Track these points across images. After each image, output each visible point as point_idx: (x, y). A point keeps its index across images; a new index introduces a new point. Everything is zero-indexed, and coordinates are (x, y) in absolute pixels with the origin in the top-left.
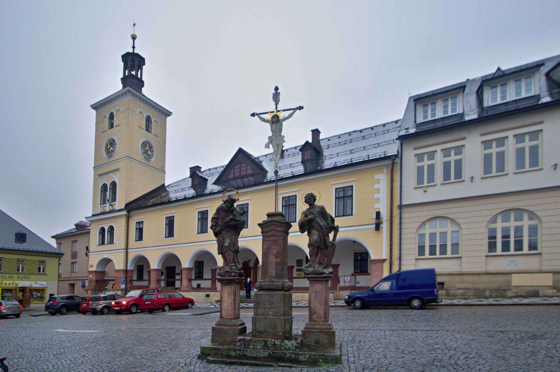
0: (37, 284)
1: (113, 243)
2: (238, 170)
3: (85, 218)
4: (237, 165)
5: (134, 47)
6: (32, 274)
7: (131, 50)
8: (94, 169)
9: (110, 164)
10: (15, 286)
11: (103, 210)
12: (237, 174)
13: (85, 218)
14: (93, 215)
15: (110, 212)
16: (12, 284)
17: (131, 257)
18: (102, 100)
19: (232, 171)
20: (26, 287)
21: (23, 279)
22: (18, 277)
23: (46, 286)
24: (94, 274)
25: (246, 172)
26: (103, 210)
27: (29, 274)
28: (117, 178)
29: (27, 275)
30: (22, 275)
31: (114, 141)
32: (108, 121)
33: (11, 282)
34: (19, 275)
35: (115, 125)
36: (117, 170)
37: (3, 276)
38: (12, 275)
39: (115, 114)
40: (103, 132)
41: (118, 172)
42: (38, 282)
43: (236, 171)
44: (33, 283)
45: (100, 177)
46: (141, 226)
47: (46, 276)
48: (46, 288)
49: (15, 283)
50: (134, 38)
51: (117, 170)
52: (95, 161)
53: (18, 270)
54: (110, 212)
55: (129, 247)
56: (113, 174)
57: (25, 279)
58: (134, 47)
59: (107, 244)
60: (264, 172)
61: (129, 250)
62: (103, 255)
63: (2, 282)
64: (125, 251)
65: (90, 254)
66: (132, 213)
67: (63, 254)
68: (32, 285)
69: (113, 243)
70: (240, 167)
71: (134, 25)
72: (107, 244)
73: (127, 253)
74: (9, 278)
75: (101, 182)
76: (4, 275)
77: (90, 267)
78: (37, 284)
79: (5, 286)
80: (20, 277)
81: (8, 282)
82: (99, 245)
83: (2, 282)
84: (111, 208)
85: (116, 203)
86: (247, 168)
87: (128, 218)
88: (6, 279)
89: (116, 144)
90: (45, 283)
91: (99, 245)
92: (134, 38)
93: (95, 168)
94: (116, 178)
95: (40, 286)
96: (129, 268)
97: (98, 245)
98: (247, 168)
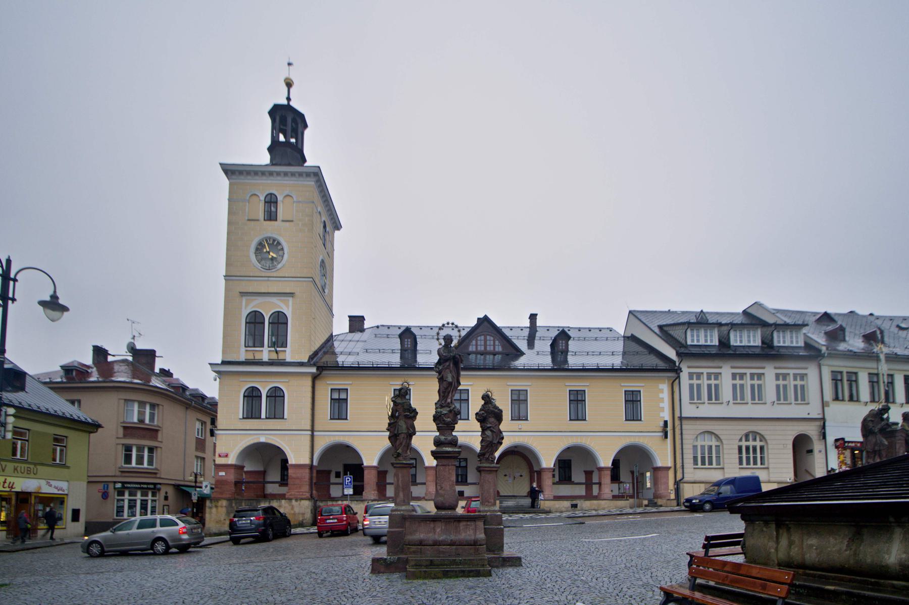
0: (51, 486)
1: (283, 418)
2: (483, 343)
3: (210, 364)
4: (481, 335)
6: (43, 464)
8: (225, 280)
9: (268, 280)
10: (8, 489)
11: (252, 358)
13: (210, 364)
14: (224, 363)
15: (271, 363)
17: (322, 444)
18: (252, 165)
19: (474, 342)
20: (30, 494)
21: (25, 475)
22: (15, 469)
23: (66, 492)
24: (232, 471)
25: (485, 348)
26: (250, 357)
27: (35, 464)
28: (288, 309)
29: (32, 466)
30: (23, 465)
31: (279, 243)
32: (262, 205)
34: (16, 465)
35: (280, 216)
36: (291, 294)
39: (280, 198)
40: (249, 220)
41: (291, 299)
42: (53, 483)
44: (43, 483)
45: (242, 296)
46: (343, 396)
47: (66, 470)
48: (65, 496)
49: (8, 482)
51: (291, 294)
52: (229, 264)
53: (14, 454)
54: (271, 363)
55: (316, 428)
56: (279, 300)
57: (29, 474)
59: (266, 418)
60: (519, 353)
61: (315, 433)
62: (256, 436)
64: (310, 433)
66: (325, 372)
67: (99, 426)
68: (40, 488)
69: (283, 418)
70: (485, 340)
72: (266, 418)
73: (312, 436)
75: (245, 308)
77: (220, 456)
78: (51, 486)
80: (19, 469)
82: (243, 418)
84: (274, 356)
85: (288, 349)
86: (494, 343)
87: (315, 378)
89: (282, 249)
90: (64, 485)
91: (243, 418)
94: (288, 308)
95: (56, 491)
96: (315, 463)
97: (241, 417)
98: (494, 343)
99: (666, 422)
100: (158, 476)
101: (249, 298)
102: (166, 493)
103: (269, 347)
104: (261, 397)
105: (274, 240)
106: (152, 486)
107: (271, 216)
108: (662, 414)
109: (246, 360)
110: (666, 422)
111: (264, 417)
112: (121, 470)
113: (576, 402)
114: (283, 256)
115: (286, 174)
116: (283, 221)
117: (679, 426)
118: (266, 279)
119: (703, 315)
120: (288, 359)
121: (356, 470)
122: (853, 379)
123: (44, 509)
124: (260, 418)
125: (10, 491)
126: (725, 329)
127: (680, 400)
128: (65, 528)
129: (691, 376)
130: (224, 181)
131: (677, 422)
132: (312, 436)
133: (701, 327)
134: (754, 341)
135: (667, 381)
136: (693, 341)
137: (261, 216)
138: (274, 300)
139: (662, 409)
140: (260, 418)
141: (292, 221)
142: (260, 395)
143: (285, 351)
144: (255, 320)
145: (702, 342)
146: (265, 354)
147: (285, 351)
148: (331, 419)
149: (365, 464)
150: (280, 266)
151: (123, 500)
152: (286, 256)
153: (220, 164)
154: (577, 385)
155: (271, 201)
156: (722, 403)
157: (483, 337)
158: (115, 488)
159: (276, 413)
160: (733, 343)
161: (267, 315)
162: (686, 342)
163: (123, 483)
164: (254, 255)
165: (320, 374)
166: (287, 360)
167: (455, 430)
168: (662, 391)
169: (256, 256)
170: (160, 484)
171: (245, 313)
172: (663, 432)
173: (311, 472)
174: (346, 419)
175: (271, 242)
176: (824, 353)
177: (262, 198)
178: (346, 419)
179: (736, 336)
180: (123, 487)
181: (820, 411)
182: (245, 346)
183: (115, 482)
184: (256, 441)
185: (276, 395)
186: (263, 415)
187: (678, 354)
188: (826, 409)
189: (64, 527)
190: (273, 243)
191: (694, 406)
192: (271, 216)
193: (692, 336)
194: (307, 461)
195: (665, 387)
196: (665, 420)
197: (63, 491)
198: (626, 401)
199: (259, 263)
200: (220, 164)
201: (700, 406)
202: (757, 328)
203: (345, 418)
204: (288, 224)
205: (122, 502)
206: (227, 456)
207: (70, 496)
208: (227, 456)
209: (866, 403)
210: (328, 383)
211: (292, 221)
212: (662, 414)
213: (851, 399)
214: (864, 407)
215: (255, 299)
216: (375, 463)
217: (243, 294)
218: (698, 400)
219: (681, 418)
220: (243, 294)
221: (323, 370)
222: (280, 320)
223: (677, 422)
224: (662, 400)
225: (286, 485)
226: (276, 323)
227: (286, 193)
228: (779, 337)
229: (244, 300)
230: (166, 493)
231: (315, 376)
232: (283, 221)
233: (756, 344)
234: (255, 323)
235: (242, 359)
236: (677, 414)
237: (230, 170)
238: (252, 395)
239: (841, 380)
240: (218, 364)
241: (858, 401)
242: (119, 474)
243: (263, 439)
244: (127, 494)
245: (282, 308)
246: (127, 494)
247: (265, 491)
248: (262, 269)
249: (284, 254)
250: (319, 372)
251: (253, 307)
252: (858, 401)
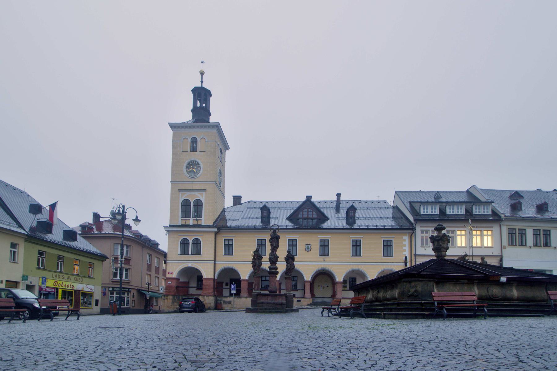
0: (87, 287)
1: (200, 254)
3: (164, 227)
5: (202, 82)
7: (199, 85)
8: (171, 183)
9: (193, 183)
11: (184, 223)
12: (305, 216)
13: (164, 227)
14: (171, 226)
15: (194, 226)
16: (70, 286)
17: (219, 268)
23: (93, 291)
24: (175, 281)
26: (184, 223)
28: (203, 197)
31: (198, 164)
32: (189, 144)
33: (69, 284)
35: (199, 149)
36: (204, 190)
37: (64, 277)
38: (70, 276)
39: (198, 140)
40: (182, 152)
41: (204, 193)
42: (88, 286)
43: (304, 213)
45: (180, 191)
46: (231, 243)
47: (93, 280)
48: (93, 293)
50: (202, 74)
51: (204, 190)
52: (173, 175)
54: (194, 226)
56: (198, 193)
58: (202, 82)
59: (192, 254)
61: (216, 262)
62: (186, 264)
63: (63, 282)
64: (213, 262)
65: (167, 261)
69: (200, 254)
71: (202, 62)
72: (192, 254)
74: (68, 279)
75: (182, 197)
76: (64, 275)
77: (169, 273)
78: (87, 287)
79: (64, 288)
81: (67, 283)
82: (180, 254)
83: (63, 282)
84: (196, 222)
85: (203, 219)
87: (216, 234)
88: (65, 280)
89: (200, 167)
90: (92, 287)
91: (180, 254)
92: (202, 74)
93: (172, 182)
94: (202, 197)
95: (89, 290)
96: (216, 278)
97: (179, 254)
99: (406, 258)
100: (130, 284)
101: (182, 192)
102: (134, 294)
103: (193, 218)
104: (189, 243)
105: (196, 162)
106: (127, 290)
107: (194, 149)
108: (404, 253)
109: (181, 224)
110: (406, 258)
111: (191, 254)
112: (112, 281)
113: (356, 246)
114: (200, 171)
115: (202, 127)
116: (200, 152)
117: (414, 260)
118: (192, 182)
119: (439, 195)
120: (203, 224)
121: (238, 281)
122: (523, 233)
123: (84, 299)
124: (189, 254)
125: (72, 290)
126: (444, 204)
127: (415, 245)
128: (93, 309)
129: (422, 232)
130: (170, 132)
131: (413, 258)
132: (215, 264)
133: (429, 204)
134: (461, 212)
135: (408, 235)
136: (424, 212)
137: (189, 149)
138: (196, 193)
139: (405, 250)
140: (189, 254)
141: (205, 152)
142: (188, 242)
143: (201, 220)
144: (186, 204)
145: (430, 213)
146: (191, 221)
147: (201, 220)
148: (224, 255)
149: (242, 278)
150: (198, 175)
151: (113, 297)
152: (202, 170)
153: (168, 123)
154: (356, 237)
155: (194, 141)
156: (430, 247)
157: (306, 210)
158: (109, 290)
159: (197, 252)
160: (448, 212)
161: (192, 201)
162: (420, 213)
163: (113, 288)
164: (185, 170)
165: (219, 231)
166: (202, 225)
167: (295, 261)
168: (405, 240)
169: (186, 170)
170: (131, 288)
171: (181, 200)
172: (404, 263)
173: (214, 283)
174: (232, 255)
175: (194, 163)
176: (503, 219)
177: (190, 140)
178: (232, 255)
179: (450, 209)
180: (114, 290)
181: (500, 252)
182: (181, 218)
183: (109, 287)
184: (187, 266)
185: (197, 243)
186: (190, 253)
187: (415, 220)
188: (503, 250)
189: (92, 308)
190: (195, 163)
191: (423, 249)
192: (194, 149)
193: (424, 209)
194: (212, 277)
195: (406, 239)
196: (406, 256)
197: (92, 290)
198: (384, 246)
199: (188, 174)
200: (168, 123)
201: (427, 249)
202: (463, 204)
203: (232, 254)
204: (202, 153)
205: (112, 298)
206: (172, 274)
207: (95, 293)
208: (172, 274)
209: (530, 247)
210: (223, 236)
211: (205, 152)
212: (404, 253)
213: (522, 245)
214: (529, 249)
215: (187, 193)
216: (247, 278)
217: (180, 190)
218: (426, 245)
219: (415, 255)
220: (180, 190)
221: (220, 230)
222: (198, 204)
223: (413, 258)
224: (405, 245)
225: (201, 289)
226: (196, 205)
227: (202, 137)
228: (476, 209)
229: (181, 193)
230: (134, 294)
231: (216, 232)
232: (200, 152)
233: (462, 214)
234: (186, 205)
235: (180, 224)
236: (413, 253)
237: (173, 126)
238: (185, 243)
239: (515, 234)
240: (167, 227)
241: (526, 245)
242: (111, 283)
243: (190, 265)
244: (115, 293)
245: (199, 197)
246: (115, 293)
247: (189, 292)
248: (189, 177)
249: (201, 169)
250: (218, 231)
251: (185, 197)
252: (526, 245)
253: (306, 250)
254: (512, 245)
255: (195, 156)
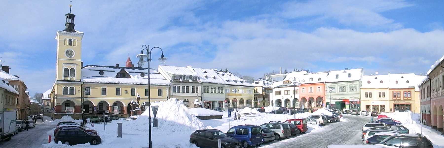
8: (59, 60)
72: (70, 94)
89: (73, 53)
94: (75, 67)
105: (71, 50)
108: (167, 95)
114: (73, 54)
138: (71, 65)
144: (66, 70)
146: (69, 79)
150: (73, 57)
168: (167, 89)
171: (63, 68)
185: (72, 90)
209: (210, 93)
222: (73, 70)
235: (63, 79)
238: (66, 89)
253: (125, 93)
254: (205, 92)
255: (70, 48)
